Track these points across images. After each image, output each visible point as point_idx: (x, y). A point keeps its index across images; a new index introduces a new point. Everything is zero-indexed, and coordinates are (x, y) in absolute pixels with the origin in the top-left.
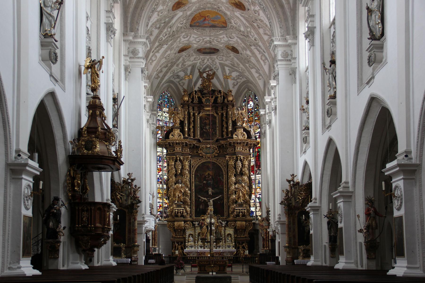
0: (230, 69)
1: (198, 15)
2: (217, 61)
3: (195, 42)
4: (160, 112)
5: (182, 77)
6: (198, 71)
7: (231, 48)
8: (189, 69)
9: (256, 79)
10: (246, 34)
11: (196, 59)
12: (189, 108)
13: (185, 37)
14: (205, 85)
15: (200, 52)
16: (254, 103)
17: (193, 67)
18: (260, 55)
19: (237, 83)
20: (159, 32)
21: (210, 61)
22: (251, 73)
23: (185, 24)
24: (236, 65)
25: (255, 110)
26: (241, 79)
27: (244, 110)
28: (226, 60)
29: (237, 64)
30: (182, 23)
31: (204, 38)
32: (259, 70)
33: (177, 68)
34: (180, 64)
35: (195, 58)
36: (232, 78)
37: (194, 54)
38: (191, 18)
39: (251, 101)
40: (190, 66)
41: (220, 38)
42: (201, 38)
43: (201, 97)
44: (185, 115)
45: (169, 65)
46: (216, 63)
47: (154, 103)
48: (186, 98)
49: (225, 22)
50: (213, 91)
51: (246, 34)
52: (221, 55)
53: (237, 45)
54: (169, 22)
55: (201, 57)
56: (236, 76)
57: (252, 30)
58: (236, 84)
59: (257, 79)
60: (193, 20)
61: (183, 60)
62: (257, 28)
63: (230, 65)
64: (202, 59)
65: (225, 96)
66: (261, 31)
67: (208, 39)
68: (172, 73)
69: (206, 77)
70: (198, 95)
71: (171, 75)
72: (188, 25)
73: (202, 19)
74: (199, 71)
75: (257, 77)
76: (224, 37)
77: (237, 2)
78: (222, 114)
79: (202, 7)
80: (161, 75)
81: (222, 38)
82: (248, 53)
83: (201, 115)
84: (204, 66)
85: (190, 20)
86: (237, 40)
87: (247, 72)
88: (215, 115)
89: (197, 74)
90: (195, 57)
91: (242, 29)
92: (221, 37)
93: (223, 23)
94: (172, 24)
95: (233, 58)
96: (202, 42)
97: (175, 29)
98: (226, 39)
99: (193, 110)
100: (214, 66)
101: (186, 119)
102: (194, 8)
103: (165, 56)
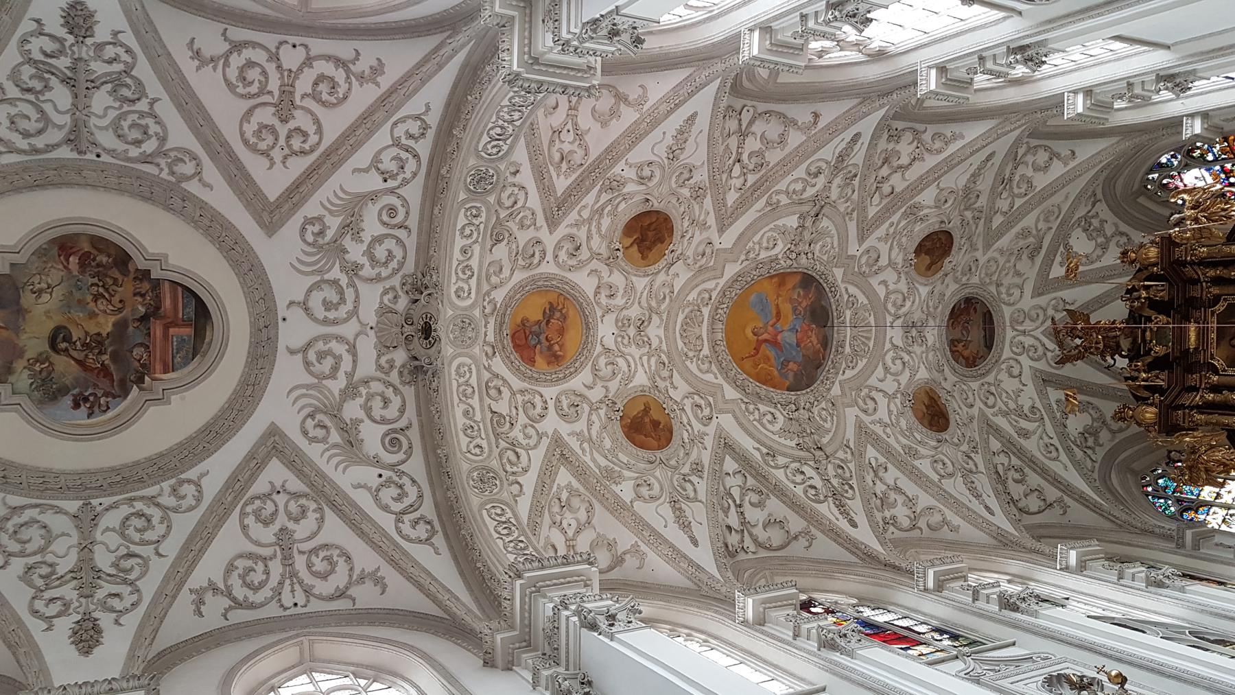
0: (1058, 259)
1: (748, 364)
2: (1027, 303)
3: (907, 374)
4: (1214, 513)
5: (1093, 420)
6: (1068, 365)
7: (927, 260)
8: (1055, 395)
9: (1074, 168)
10: (805, 208)
11: (1016, 372)
12: (1182, 407)
13: (871, 404)
14: (1101, 346)
15: (984, 358)
16: (1187, 167)
17: (1046, 381)
18: (926, 156)
19: (1122, 234)
20: (777, 497)
21: (1028, 325)
22: (1052, 190)
23: (776, 407)
24: (1031, 240)
25: (1210, 157)
26: (1103, 222)
27: (1186, 196)
28: (1018, 274)
29: (1025, 233)
30: (769, 417)
31: (888, 346)
32: (992, 155)
33: (1035, 438)
34: (1024, 424)
35: (1011, 376)
36: (1099, 252)
37: (990, 378)
38: (753, 386)
39: (1182, 181)
40: (1042, 394)
41: (888, 294)
42: (891, 354)
43: (1149, 359)
44: (1207, 424)
45: (1015, 461)
46: (1034, 307)
47: (1157, 530)
48: (1150, 413)
49: (775, 280)
50: (1134, 317)
51: (805, 208)
52: (999, 293)
53: (904, 240)
54: (743, 459)
55: (1007, 353)
56: (1090, 238)
57: (782, 186)
58: (1124, 240)
59: (1072, 164)
60: (766, 380)
61: (1005, 414)
62: (763, 171)
63: (1039, 259)
64: (1015, 353)
65: (1146, 273)
66: (774, 157)
67: (895, 335)
68: (1054, 454)
69: (1078, 341)
70: (1138, 371)
71: (1063, 457)
72: (792, 396)
73: (769, 351)
74: (1062, 362)
75: (1066, 164)
76: (884, 282)
77: (629, 241)
78: (1217, 281)
79: (706, 351)
80: (1052, 493)
81: (887, 287)
82: (927, 197)
83: (1219, 363)
84: (1051, 345)
85: (763, 390)
86: (879, 239)
87: (1056, 199)
88: (1220, 307)
89: (1081, 371)
90: (1003, 376)
91: (792, 222)
92: (881, 291)
93: (781, 284)
94: (758, 449)
95: (1001, 252)
96: (909, 353)
97: (788, 442)
98: (890, 276)
99: (1195, 389)
100: (1050, 312)
101: (1226, 420)
102: (709, 377)
103: (935, 477)
